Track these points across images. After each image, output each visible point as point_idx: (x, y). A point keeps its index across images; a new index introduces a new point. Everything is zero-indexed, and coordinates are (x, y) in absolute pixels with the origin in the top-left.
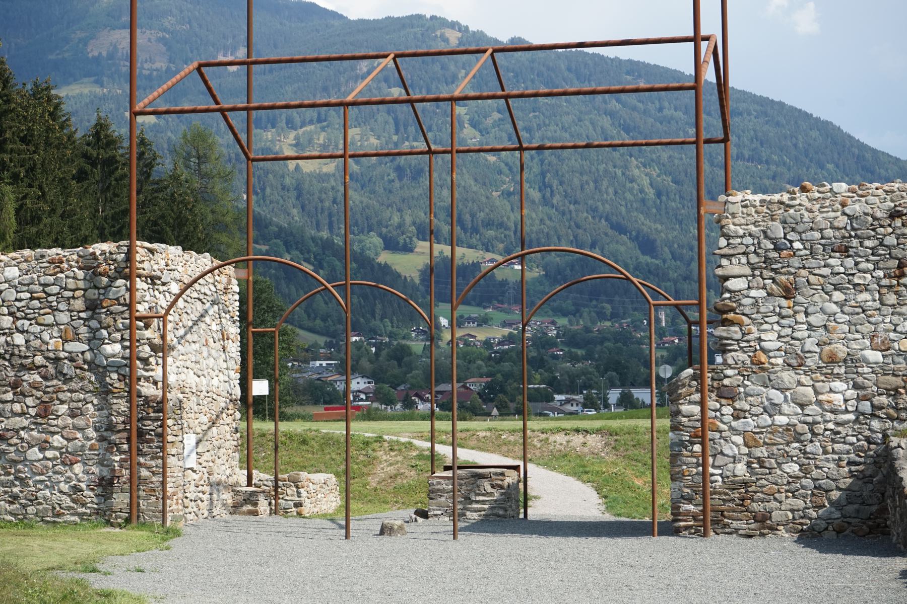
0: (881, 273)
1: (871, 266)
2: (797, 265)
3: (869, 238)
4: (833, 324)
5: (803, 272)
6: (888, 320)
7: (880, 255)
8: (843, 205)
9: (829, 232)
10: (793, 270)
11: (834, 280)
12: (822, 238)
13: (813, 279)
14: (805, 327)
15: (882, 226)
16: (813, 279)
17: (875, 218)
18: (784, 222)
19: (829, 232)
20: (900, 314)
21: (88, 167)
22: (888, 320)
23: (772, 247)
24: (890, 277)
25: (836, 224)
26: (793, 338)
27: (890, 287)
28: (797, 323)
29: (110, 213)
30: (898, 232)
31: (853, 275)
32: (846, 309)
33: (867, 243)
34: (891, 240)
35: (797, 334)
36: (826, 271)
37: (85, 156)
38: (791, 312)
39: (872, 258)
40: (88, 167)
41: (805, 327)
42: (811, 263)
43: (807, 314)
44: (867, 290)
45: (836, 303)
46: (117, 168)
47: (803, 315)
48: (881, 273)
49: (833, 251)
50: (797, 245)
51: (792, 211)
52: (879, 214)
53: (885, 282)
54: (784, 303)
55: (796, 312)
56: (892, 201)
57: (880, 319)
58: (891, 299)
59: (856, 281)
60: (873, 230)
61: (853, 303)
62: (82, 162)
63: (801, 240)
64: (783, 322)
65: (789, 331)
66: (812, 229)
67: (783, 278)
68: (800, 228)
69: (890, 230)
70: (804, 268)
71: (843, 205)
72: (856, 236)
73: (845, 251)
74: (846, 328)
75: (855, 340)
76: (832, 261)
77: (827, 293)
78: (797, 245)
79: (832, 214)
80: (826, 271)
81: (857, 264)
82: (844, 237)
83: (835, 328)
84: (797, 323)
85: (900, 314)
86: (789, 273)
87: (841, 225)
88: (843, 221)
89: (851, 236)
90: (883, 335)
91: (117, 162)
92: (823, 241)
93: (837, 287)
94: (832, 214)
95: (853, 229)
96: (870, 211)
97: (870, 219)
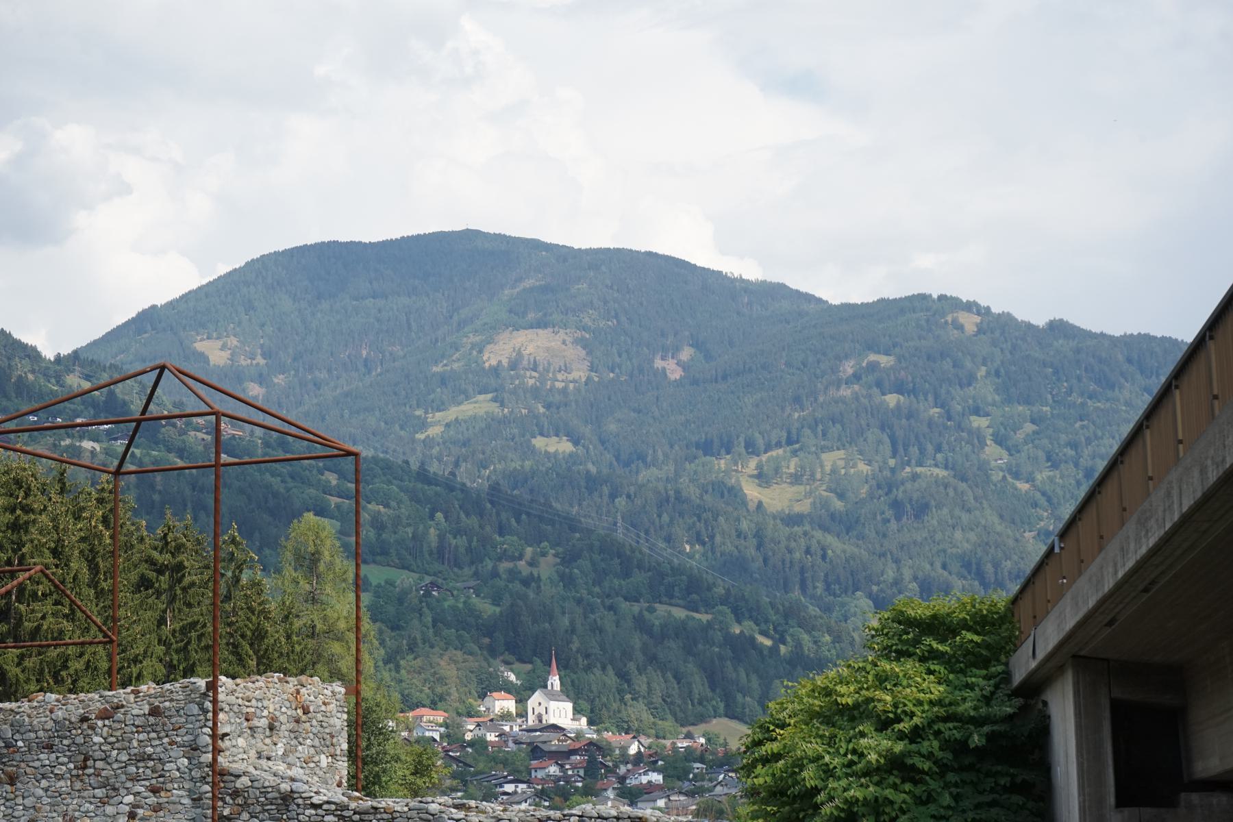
0: (71, 766)
1: (66, 760)
2: (18, 759)
3: (66, 738)
4: (40, 805)
5: (23, 765)
6: (75, 802)
7: (72, 751)
8: (51, 711)
9: (41, 734)
10: (14, 763)
11: (42, 771)
12: (37, 738)
13: (28, 770)
14: (21, 807)
15: (75, 729)
16: (28, 770)
17: (71, 723)
18: (12, 725)
19: (41, 734)
20: (84, 798)
21: (152, 575)
22: (75, 802)
23: (3, 745)
24: (78, 769)
25: (46, 727)
26: (13, 817)
27: (78, 776)
28: (16, 804)
29: (177, 626)
30: (85, 733)
31: (55, 766)
32: (49, 793)
33: (66, 742)
34: (80, 740)
35: (16, 814)
36: (37, 764)
37: (151, 562)
38: (13, 796)
39: (68, 753)
40: (152, 575)
41: (21, 807)
42: (29, 757)
43: (24, 798)
44: (63, 778)
45: (43, 789)
46: (184, 576)
47: (21, 798)
48: (71, 766)
49: (43, 748)
50: (20, 744)
51: (18, 717)
52: (73, 720)
53: (74, 772)
54: (8, 788)
55: (16, 796)
56: (83, 709)
57: (70, 801)
58: (78, 785)
59: (56, 771)
60: (70, 731)
61: (53, 789)
62: (144, 568)
63: (22, 740)
64: (7, 804)
65: (10, 811)
66: (30, 731)
67: (10, 769)
68: (22, 730)
69: (80, 731)
70: (23, 761)
71: (51, 711)
72: (58, 737)
73: (50, 747)
74: (48, 808)
75: (53, 818)
76: (42, 756)
77: (37, 781)
78: (20, 744)
79: (43, 719)
80: (37, 764)
81: (57, 758)
82: (50, 737)
83: (40, 808)
84: (16, 804)
85: (84, 798)
86: (12, 766)
87: (49, 728)
88: (50, 725)
89: (55, 737)
90: (70, 813)
91: (185, 568)
92: (37, 740)
93: (44, 776)
94: (43, 719)
95: (57, 731)
96: (68, 717)
97: (67, 722)
